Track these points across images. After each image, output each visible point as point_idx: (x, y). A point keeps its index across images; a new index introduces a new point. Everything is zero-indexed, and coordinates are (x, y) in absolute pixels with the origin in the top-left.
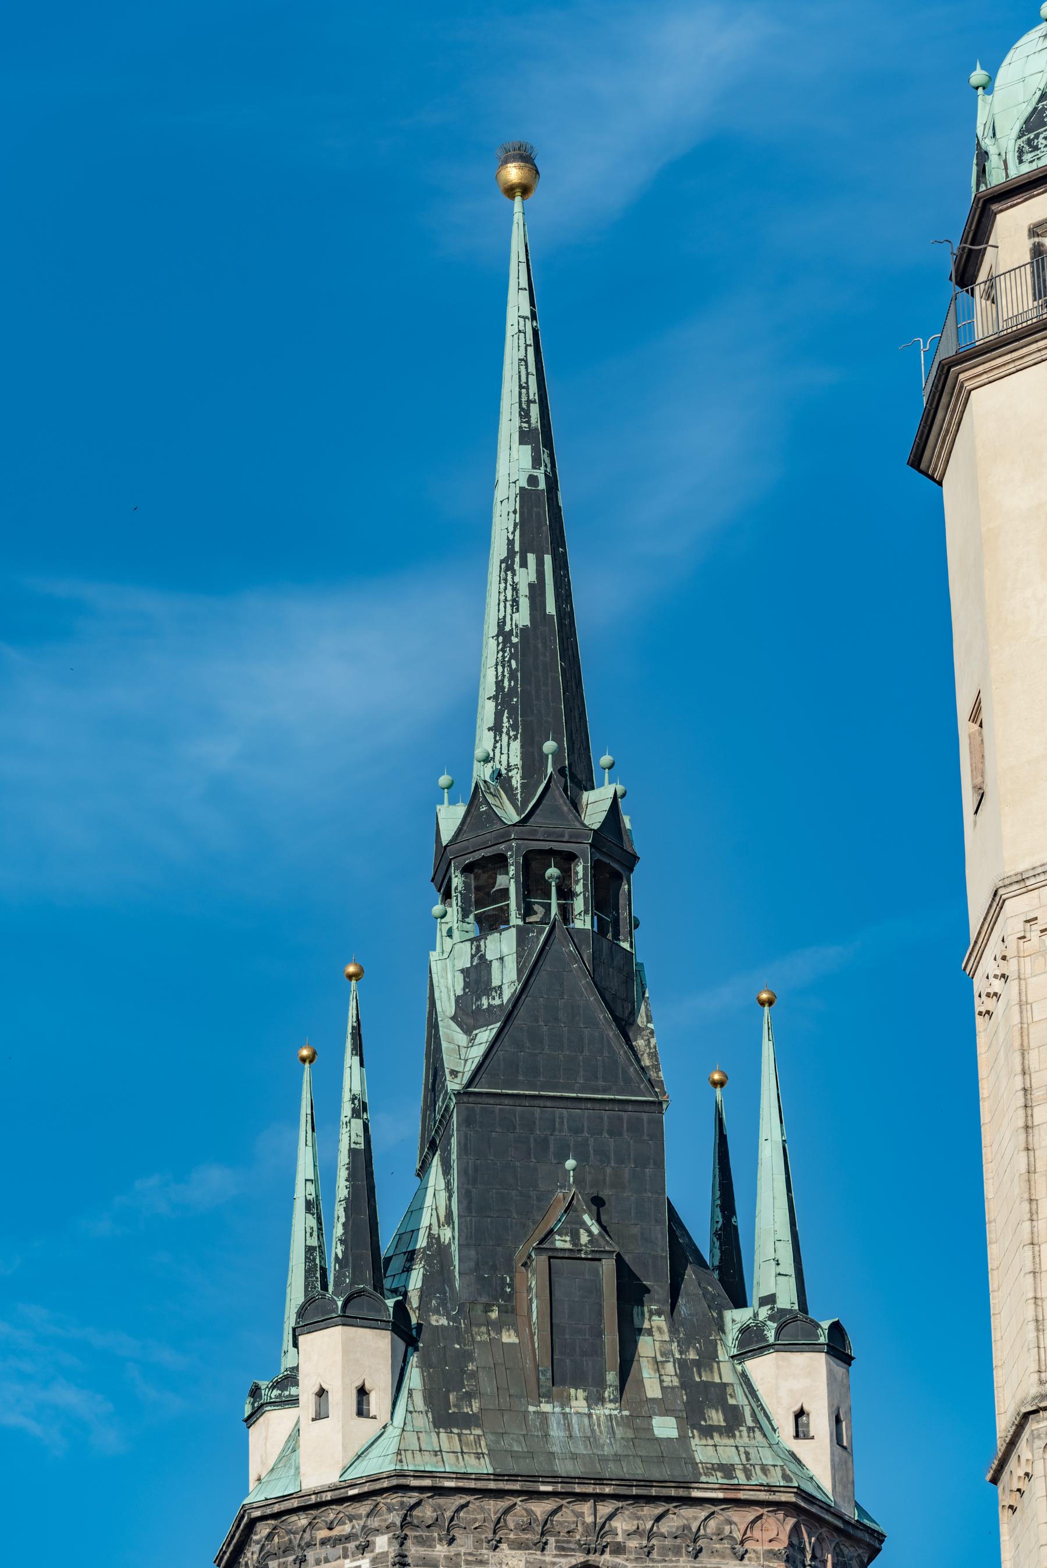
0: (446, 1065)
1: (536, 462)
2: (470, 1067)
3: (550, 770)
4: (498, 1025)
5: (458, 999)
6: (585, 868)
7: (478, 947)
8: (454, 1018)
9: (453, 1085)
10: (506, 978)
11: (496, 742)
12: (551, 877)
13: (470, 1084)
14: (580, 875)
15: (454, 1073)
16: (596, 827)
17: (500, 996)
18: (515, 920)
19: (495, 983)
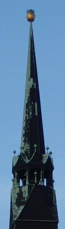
0: (13, 215)
1: (34, 83)
2: (18, 215)
3: (35, 151)
4: (24, 205)
5: (16, 199)
6: (42, 172)
7: (20, 189)
8: (15, 204)
9: (15, 219)
10: (26, 195)
11: (25, 144)
12: (35, 174)
13: (19, 218)
14: (41, 173)
15: (15, 216)
16: (45, 163)
17: (25, 199)
18: (27, 183)
19: (24, 196)
